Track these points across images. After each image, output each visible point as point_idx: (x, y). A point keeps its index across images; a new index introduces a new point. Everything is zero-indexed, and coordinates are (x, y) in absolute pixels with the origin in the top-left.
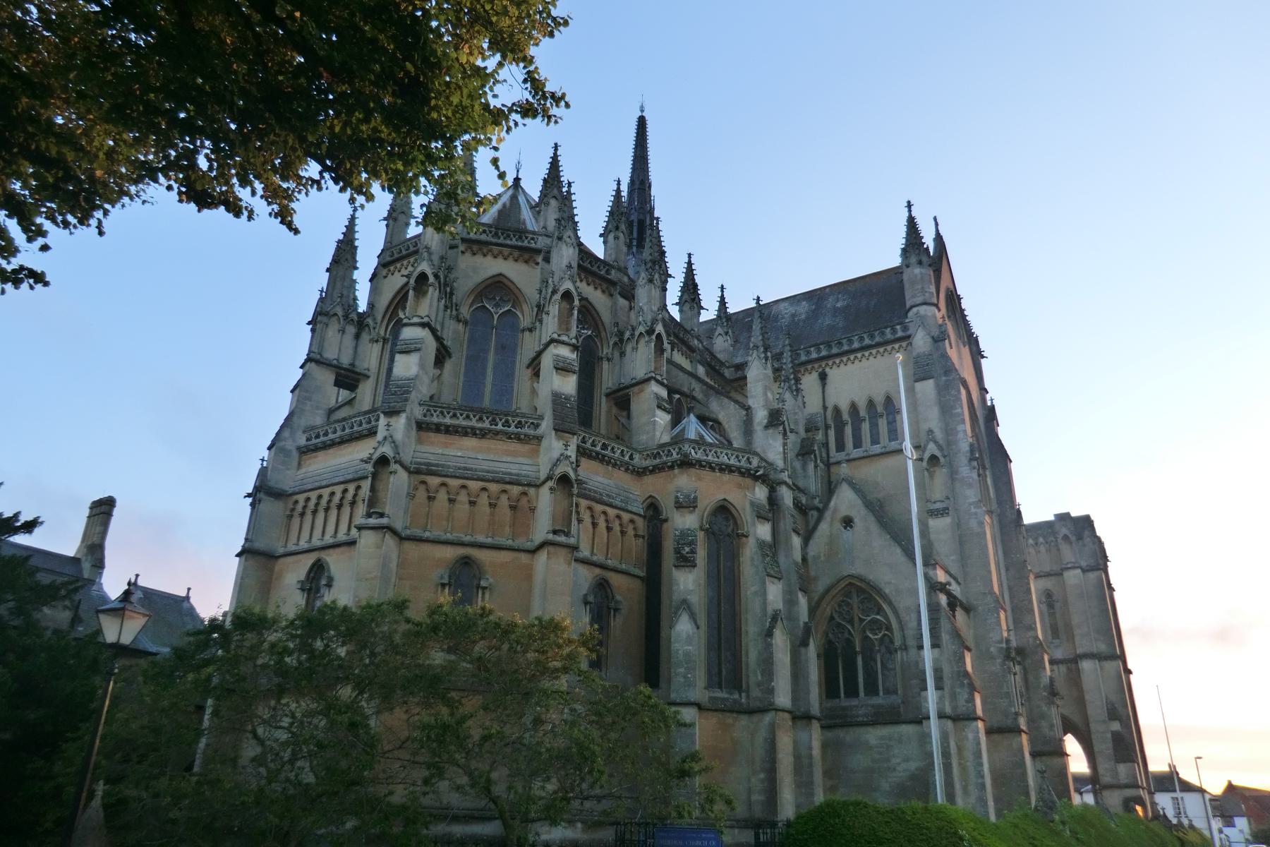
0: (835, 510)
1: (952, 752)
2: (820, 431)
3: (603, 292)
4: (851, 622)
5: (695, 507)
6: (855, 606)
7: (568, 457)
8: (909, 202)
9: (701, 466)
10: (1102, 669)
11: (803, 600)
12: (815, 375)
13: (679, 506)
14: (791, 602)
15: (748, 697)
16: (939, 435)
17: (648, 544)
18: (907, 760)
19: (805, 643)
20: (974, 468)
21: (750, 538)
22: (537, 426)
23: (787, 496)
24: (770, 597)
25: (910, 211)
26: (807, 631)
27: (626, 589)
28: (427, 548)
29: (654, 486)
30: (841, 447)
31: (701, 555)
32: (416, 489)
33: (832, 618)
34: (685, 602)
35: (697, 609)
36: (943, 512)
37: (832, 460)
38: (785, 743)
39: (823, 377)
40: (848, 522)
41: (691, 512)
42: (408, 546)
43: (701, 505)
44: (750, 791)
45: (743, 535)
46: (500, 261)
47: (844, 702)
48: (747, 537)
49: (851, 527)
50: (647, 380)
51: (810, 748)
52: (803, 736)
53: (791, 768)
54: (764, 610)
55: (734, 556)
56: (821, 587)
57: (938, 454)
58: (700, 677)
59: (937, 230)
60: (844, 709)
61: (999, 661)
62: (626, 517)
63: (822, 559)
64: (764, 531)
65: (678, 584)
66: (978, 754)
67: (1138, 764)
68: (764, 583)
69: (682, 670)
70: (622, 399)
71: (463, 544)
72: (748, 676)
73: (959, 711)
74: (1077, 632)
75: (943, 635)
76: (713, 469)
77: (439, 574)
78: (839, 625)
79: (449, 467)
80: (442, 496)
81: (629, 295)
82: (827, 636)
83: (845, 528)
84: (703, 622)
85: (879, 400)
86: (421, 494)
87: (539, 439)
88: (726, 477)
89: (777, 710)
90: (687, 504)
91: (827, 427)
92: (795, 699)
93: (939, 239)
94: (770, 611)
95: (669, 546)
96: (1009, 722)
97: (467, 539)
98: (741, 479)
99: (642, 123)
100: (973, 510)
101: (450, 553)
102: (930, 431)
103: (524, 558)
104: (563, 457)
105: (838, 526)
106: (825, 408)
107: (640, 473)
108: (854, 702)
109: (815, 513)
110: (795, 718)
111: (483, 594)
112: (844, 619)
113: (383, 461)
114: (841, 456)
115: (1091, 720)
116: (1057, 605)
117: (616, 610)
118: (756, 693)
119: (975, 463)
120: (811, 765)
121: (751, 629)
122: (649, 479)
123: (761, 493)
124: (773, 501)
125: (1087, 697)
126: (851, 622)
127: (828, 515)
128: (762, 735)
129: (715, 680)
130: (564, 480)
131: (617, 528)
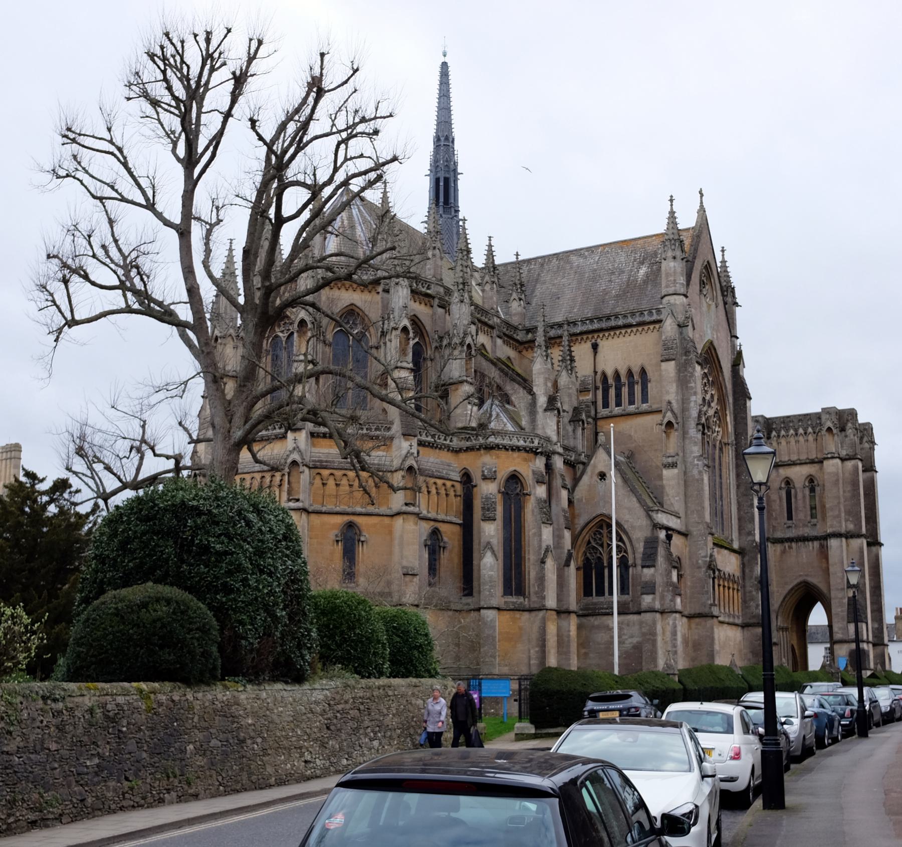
0: (595, 466)
1: (658, 632)
2: (591, 392)
4: (602, 545)
5: (495, 479)
6: (605, 535)
7: (412, 454)
9: (499, 448)
10: (848, 545)
11: (567, 535)
12: (588, 345)
13: (485, 478)
14: (558, 537)
15: (529, 600)
16: (675, 405)
17: (464, 500)
18: (632, 637)
19: (567, 564)
20: (700, 430)
21: (532, 496)
22: (389, 429)
23: (558, 463)
24: (544, 537)
25: (672, 205)
26: (570, 556)
27: (451, 535)
28: (326, 518)
29: (468, 461)
30: (606, 405)
31: (500, 509)
32: (314, 479)
33: (589, 542)
34: (489, 543)
35: (496, 549)
36: (673, 465)
37: (599, 416)
38: (552, 629)
39: (595, 347)
40: (603, 476)
41: (492, 482)
42: (313, 516)
43: (499, 476)
44: (529, 658)
45: (527, 494)
46: (350, 292)
47: (595, 599)
48: (529, 495)
49: (605, 479)
50: (461, 382)
51: (569, 631)
52: (564, 623)
53: (555, 644)
54: (540, 547)
55: (520, 509)
56: (581, 522)
57: (673, 421)
58: (499, 589)
59: (702, 202)
60: (595, 604)
61: (704, 569)
62: (449, 484)
63: (584, 501)
64: (541, 491)
65: (485, 532)
66: (674, 633)
67: (867, 623)
68: (541, 528)
69: (487, 587)
70: (444, 390)
71: (348, 514)
72: (529, 587)
73: (665, 607)
74: (829, 514)
75: (659, 558)
76: (507, 450)
77: (332, 535)
78: (594, 548)
79: (333, 462)
80: (331, 482)
81: (445, 306)
82: (586, 555)
83: (601, 480)
84: (500, 555)
85: (636, 370)
86: (318, 481)
87: (392, 438)
88: (516, 454)
89: (547, 610)
90: (489, 478)
91: (596, 388)
92: (559, 599)
93: (702, 210)
94: (544, 546)
95: (477, 505)
96: (706, 610)
97: (349, 510)
99: (444, 65)
100: (696, 462)
101: (340, 520)
102: (669, 403)
103: (387, 520)
104: (408, 454)
105: (596, 478)
106: (596, 372)
107: (457, 451)
108: (601, 599)
109: (581, 466)
110: (559, 612)
111: (362, 545)
112: (597, 543)
113: (294, 463)
114: (603, 412)
115: (832, 588)
116: (818, 489)
117: (444, 548)
118: (534, 598)
119: (700, 427)
120: (569, 641)
121: (531, 558)
122: (463, 456)
123: (539, 463)
124: (549, 467)
125: (831, 570)
126: (602, 545)
127: (589, 469)
128: (537, 624)
129: (507, 591)
130: (410, 469)
131: (443, 492)
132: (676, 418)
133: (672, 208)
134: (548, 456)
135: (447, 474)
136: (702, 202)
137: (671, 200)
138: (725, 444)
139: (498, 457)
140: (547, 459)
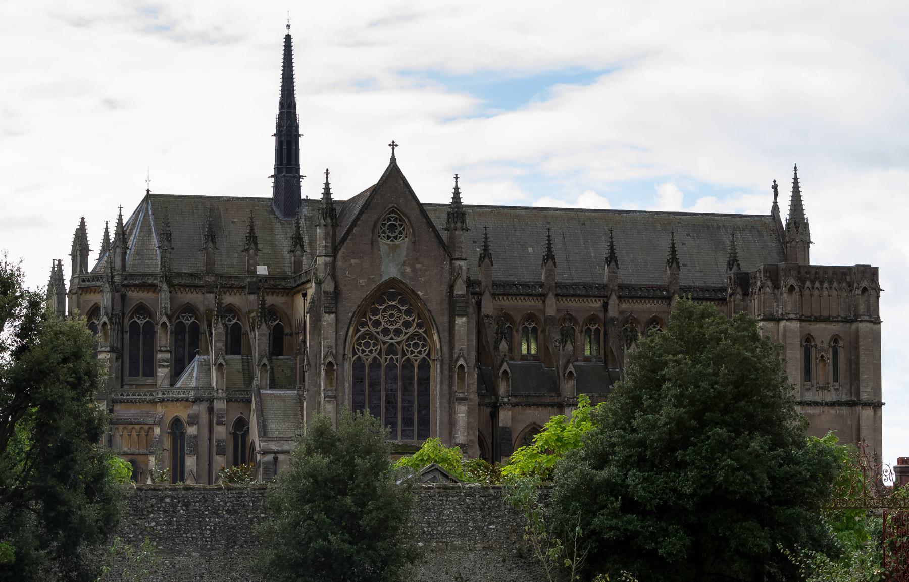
3: (153, 292)
8: (327, 170)
12: (301, 296)
59: (393, 154)
76: (172, 401)
88: (178, 404)
99: (288, 38)
134: (211, 401)
135: (144, 420)
136: (393, 154)
137: (327, 173)
138: (433, 360)
139: (166, 407)
140: (210, 404)
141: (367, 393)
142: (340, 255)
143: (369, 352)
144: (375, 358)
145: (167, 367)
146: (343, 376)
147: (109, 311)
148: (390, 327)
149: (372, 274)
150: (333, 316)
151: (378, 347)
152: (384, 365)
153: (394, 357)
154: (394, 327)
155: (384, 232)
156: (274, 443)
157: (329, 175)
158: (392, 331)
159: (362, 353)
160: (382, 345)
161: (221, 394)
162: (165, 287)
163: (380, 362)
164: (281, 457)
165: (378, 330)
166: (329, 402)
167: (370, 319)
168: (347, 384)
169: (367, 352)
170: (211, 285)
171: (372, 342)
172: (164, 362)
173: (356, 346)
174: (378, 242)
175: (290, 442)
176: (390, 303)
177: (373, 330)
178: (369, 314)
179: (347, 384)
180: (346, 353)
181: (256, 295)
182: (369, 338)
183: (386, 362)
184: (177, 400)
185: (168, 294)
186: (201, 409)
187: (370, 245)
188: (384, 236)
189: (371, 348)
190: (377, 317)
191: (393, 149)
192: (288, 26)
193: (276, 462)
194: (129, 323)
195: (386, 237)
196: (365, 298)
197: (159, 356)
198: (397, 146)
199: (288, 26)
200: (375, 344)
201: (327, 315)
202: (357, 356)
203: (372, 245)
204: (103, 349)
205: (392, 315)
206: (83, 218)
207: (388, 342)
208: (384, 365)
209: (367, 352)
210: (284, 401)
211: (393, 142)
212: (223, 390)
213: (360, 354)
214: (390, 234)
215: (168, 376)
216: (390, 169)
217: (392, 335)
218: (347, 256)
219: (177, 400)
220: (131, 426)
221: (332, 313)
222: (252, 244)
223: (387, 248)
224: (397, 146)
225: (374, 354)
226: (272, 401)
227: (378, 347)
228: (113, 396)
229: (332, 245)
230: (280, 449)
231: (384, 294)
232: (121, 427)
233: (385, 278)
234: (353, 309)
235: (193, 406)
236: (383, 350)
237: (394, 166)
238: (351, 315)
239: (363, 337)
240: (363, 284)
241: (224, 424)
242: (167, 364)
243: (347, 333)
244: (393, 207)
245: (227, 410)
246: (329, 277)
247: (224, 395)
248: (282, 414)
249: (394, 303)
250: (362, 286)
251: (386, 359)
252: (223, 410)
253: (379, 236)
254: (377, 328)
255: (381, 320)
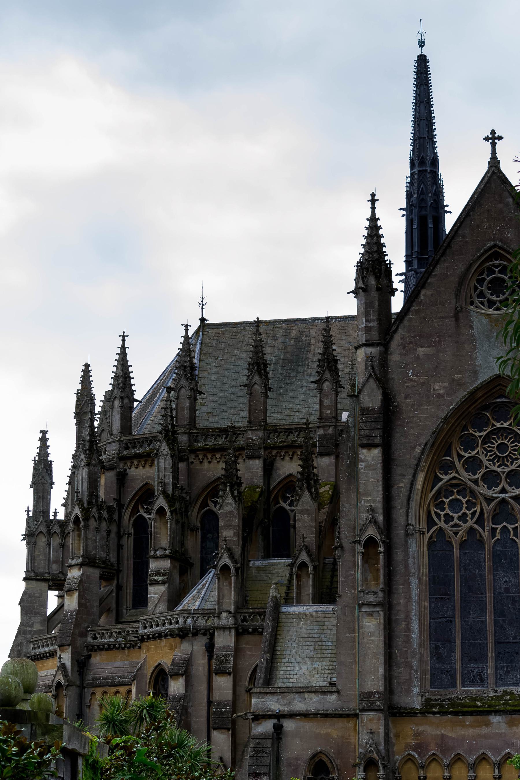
8: (373, 195)
25: (373, 208)
59: (494, 153)
76: (154, 638)
88: (163, 643)
98: (172, 640)
132: (235, 562)
133: (373, 213)
136: (494, 153)
137: (373, 201)
141: (457, 596)
142: (395, 343)
143: (459, 518)
144: (471, 529)
145: (163, 583)
146: (407, 566)
147: (85, 499)
148: (499, 470)
149: (459, 373)
150: (377, 452)
151: (478, 508)
152: (489, 542)
153: (509, 526)
154: (508, 469)
155: (481, 295)
156: (275, 698)
157: (377, 204)
158: (503, 476)
159: (446, 522)
160: (484, 504)
161: (226, 620)
162: (165, 448)
163: (481, 536)
164: (289, 725)
165: (478, 476)
166: (370, 614)
167: (460, 457)
168: (414, 582)
169: (456, 520)
170: (255, 444)
171: (464, 500)
172: (159, 574)
173: (433, 509)
174: (468, 312)
175: (306, 695)
176: (498, 425)
177: (465, 476)
178: (457, 448)
179: (414, 582)
180: (412, 521)
181: (333, 457)
182: (458, 493)
183: (494, 536)
184: (160, 636)
185: (169, 460)
186: (195, 648)
187: (453, 319)
188: (482, 303)
189: (464, 510)
190: (473, 453)
191: (494, 145)
192: (422, 44)
193: (278, 734)
194: (132, 520)
195: (486, 304)
196: (445, 418)
197: (154, 565)
198: (500, 138)
199: (422, 44)
200: (470, 505)
201: (365, 451)
202: (435, 528)
203: (457, 319)
204: (75, 561)
205: (502, 447)
206: (87, 366)
207: (497, 498)
208: (489, 542)
209: (456, 520)
210: (322, 625)
211: (493, 132)
212: (230, 612)
213: (441, 524)
214: (494, 298)
215: (165, 598)
216: (486, 179)
217: (503, 484)
218: (411, 343)
219: (160, 636)
220: (113, 689)
221: (375, 446)
222: (327, 372)
223: (485, 321)
224: (500, 138)
225: (470, 523)
226: (298, 625)
227: (478, 508)
228: (90, 639)
229: (380, 324)
230: (287, 709)
231: (486, 408)
232: (99, 691)
233: (484, 376)
234: (423, 440)
235: (181, 643)
236: (486, 514)
237: (493, 173)
238: (418, 450)
239: (446, 491)
240: (442, 392)
241: (229, 674)
242: (163, 578)
243: (412, 485)
244: (495, 246)
245: (237, 650)
246: (372, 382)
247: (232, 621)
248: (312, 648)
249: (506, 425)
250: (439, 395)
251: (494, 530)
252: (229, 648)
253: (472, 303)
254: (475, 474)
255: (482, 457)
